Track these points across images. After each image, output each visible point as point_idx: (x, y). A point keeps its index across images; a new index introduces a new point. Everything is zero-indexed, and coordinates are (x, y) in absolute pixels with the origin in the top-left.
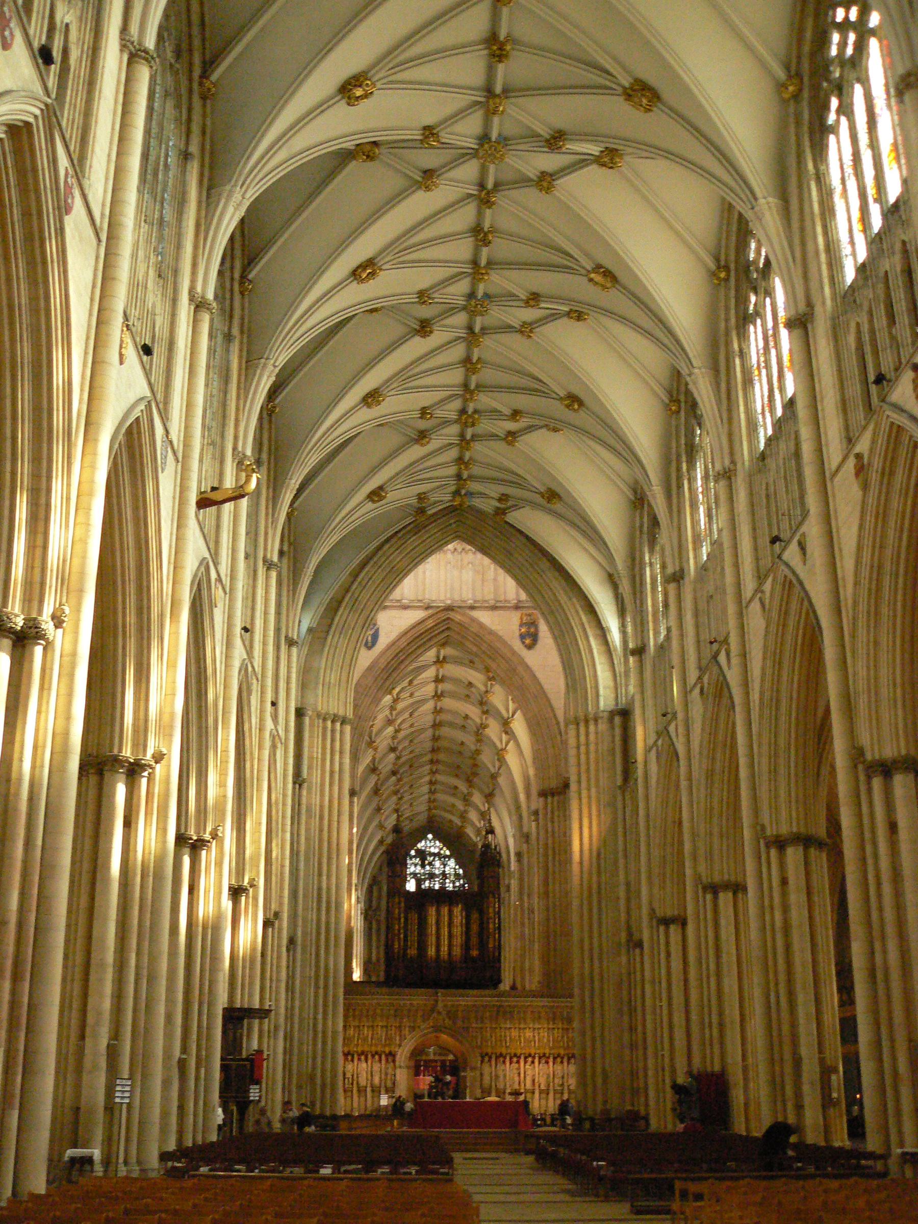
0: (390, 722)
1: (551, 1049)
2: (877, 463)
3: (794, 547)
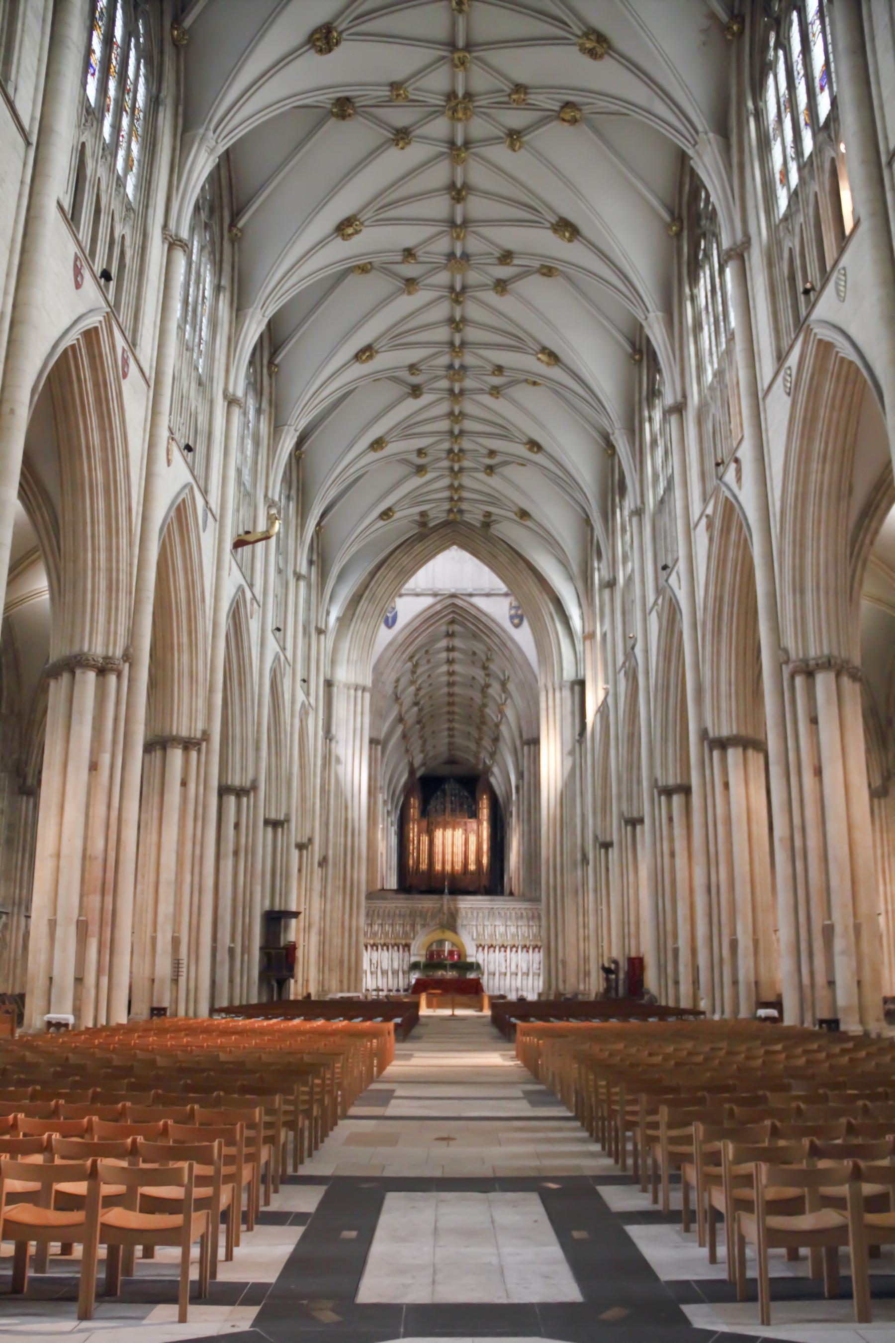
0: (412, 682)
1: (530, 941)
2: (718, 524)
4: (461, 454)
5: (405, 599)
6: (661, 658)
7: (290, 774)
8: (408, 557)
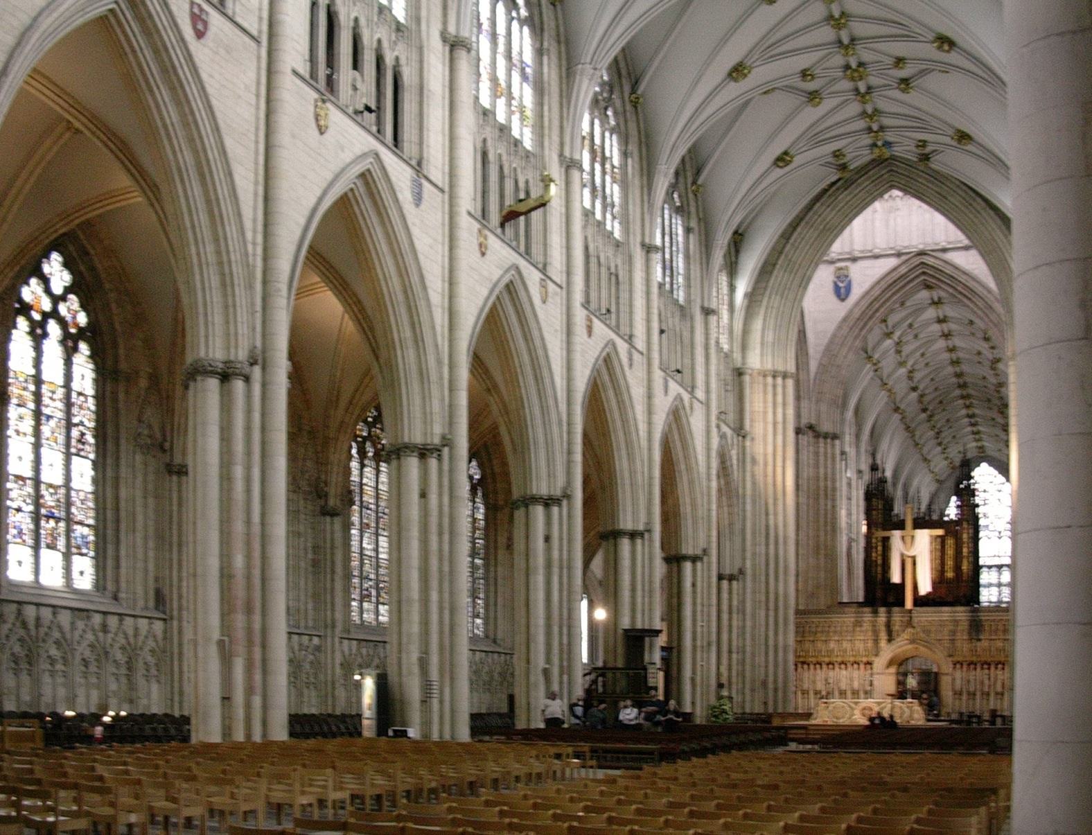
4: (861, 69)
5: (860, 264)
7: (651, 478)
8: (832, 210)
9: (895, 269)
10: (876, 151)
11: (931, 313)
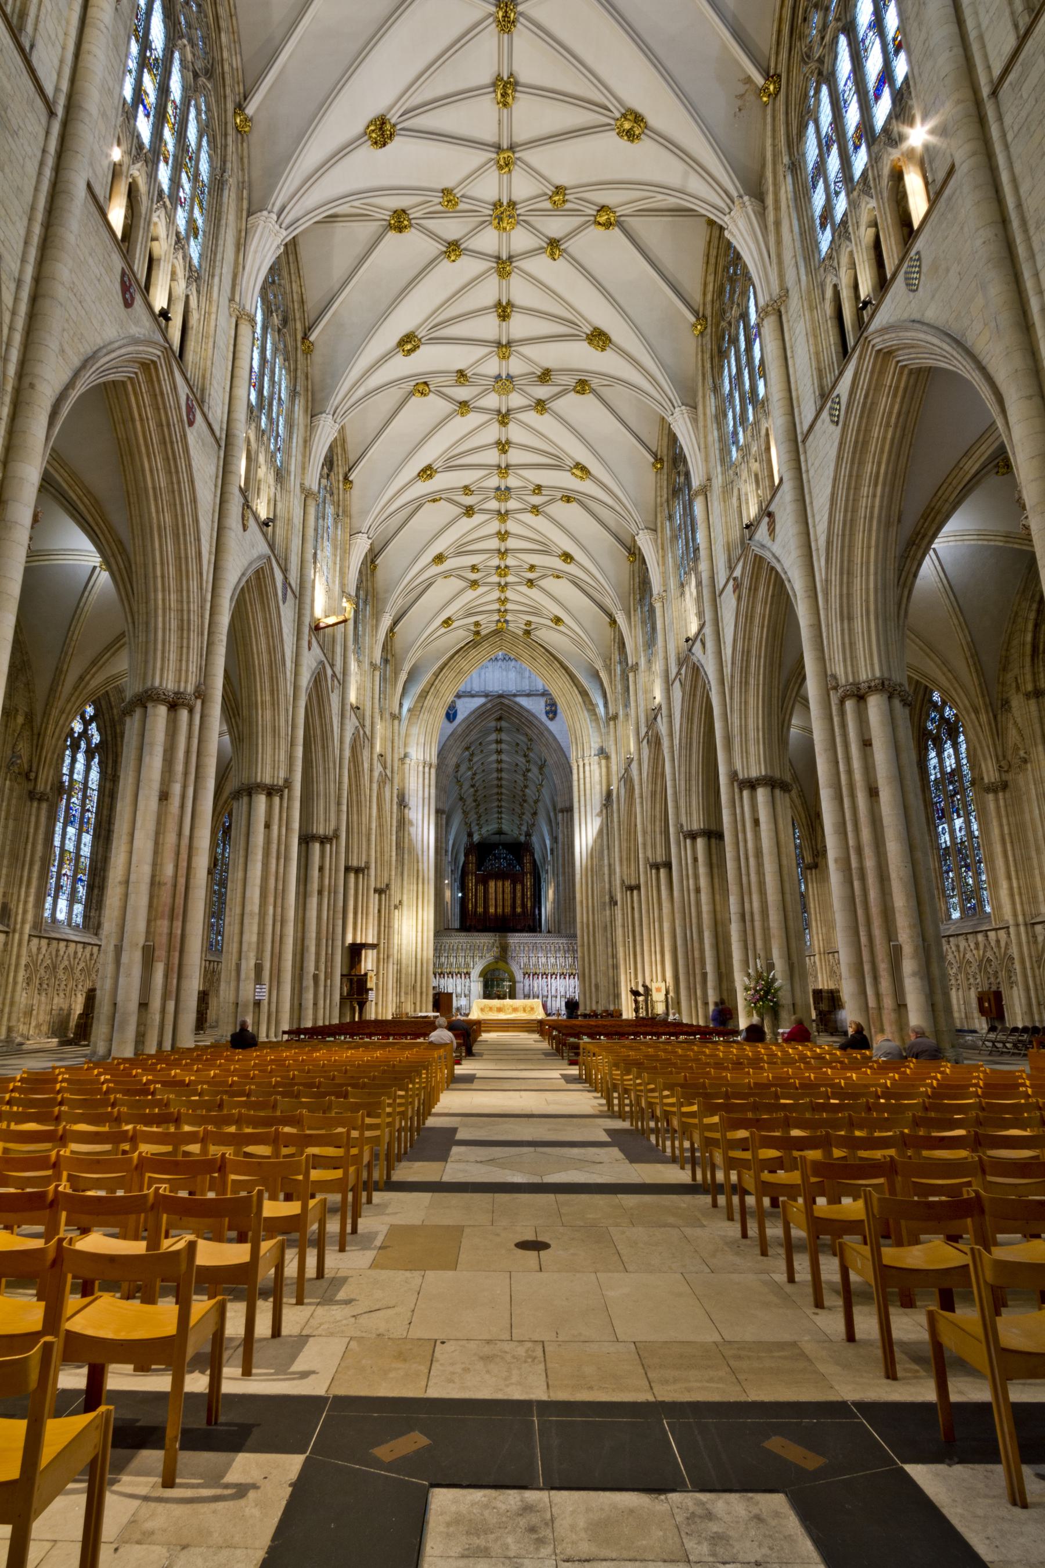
0: (470, 769)
2: (746, 583)
3: (698, 644)
6: (685, 720)
7: (370, 829)
9: (484, 705)
10: (500, 625)
11: (493, 737)
